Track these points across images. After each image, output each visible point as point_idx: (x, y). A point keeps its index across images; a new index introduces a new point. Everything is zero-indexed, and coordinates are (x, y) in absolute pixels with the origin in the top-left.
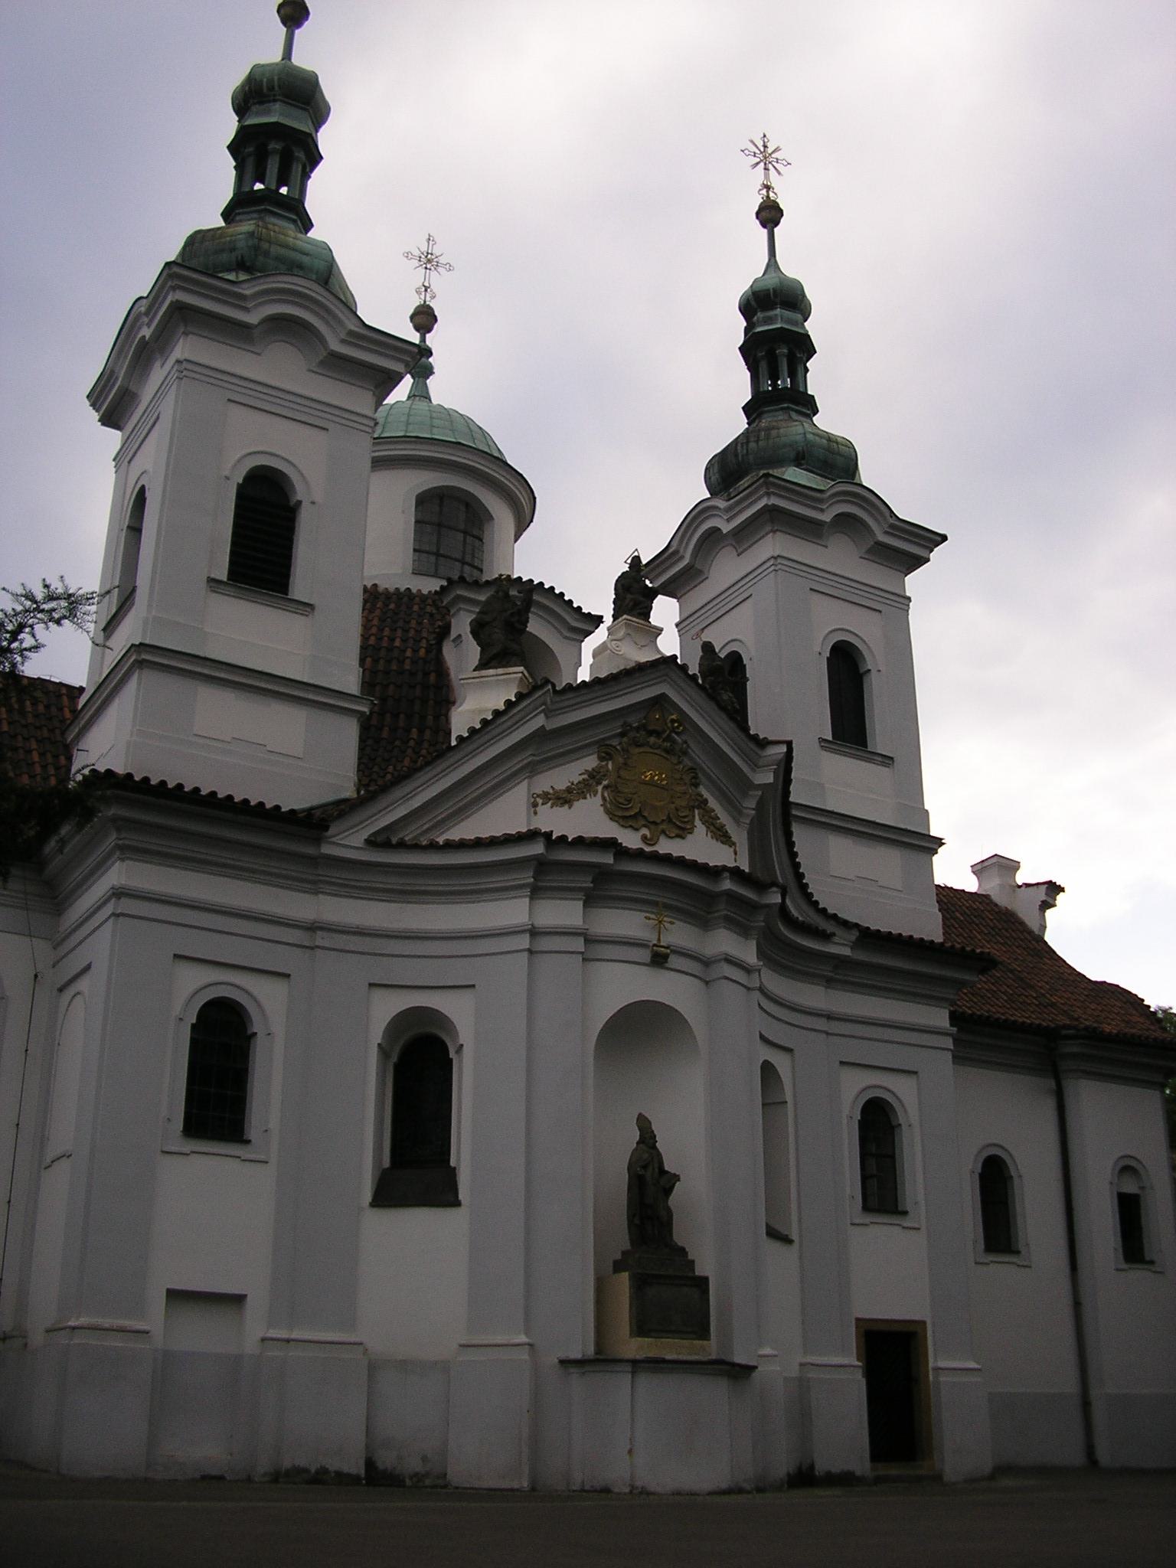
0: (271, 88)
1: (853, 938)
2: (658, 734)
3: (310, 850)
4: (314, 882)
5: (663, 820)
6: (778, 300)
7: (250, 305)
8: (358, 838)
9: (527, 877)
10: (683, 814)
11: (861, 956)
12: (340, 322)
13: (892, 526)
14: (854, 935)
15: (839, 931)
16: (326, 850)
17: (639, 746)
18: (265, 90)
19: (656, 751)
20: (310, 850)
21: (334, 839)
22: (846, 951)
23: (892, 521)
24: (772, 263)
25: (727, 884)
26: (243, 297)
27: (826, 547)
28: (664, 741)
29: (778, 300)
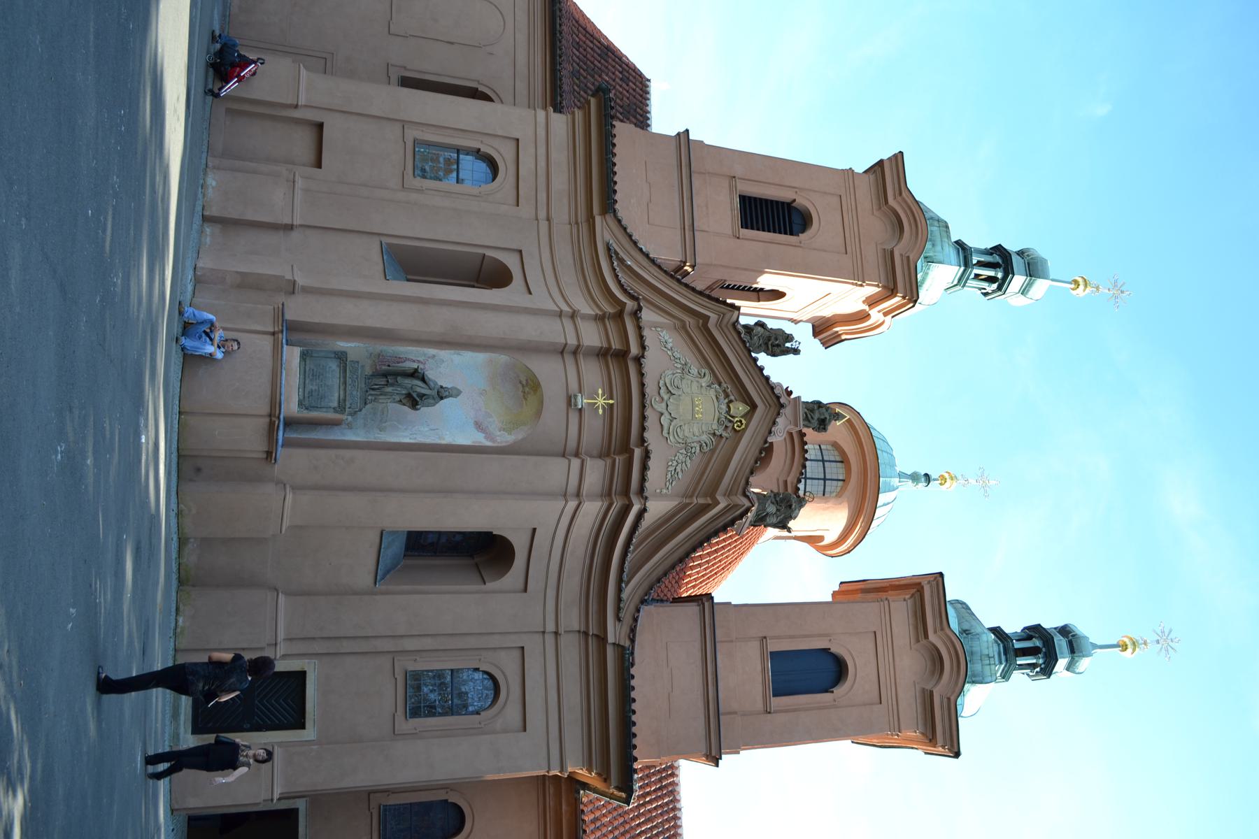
0: (1028, 256)
1: (622, 643)
2: (728, 412)
4: (577, 223)
6: (1070, 638)
7: (899, 198)
8: (608, 237)
9: (609, 309)
13: (949, 699)
15: (625, 629)
16: (598, 219)
17: (717, 398)
18: (1026, 254)
19: (717, 411)
21: (605, 223)
22: (611, 639)
23: (952, 698)
24: (1095, 646)
26: (900, 194)
27: (911, 648)
28: (726, 418)
29: (1070, 638)
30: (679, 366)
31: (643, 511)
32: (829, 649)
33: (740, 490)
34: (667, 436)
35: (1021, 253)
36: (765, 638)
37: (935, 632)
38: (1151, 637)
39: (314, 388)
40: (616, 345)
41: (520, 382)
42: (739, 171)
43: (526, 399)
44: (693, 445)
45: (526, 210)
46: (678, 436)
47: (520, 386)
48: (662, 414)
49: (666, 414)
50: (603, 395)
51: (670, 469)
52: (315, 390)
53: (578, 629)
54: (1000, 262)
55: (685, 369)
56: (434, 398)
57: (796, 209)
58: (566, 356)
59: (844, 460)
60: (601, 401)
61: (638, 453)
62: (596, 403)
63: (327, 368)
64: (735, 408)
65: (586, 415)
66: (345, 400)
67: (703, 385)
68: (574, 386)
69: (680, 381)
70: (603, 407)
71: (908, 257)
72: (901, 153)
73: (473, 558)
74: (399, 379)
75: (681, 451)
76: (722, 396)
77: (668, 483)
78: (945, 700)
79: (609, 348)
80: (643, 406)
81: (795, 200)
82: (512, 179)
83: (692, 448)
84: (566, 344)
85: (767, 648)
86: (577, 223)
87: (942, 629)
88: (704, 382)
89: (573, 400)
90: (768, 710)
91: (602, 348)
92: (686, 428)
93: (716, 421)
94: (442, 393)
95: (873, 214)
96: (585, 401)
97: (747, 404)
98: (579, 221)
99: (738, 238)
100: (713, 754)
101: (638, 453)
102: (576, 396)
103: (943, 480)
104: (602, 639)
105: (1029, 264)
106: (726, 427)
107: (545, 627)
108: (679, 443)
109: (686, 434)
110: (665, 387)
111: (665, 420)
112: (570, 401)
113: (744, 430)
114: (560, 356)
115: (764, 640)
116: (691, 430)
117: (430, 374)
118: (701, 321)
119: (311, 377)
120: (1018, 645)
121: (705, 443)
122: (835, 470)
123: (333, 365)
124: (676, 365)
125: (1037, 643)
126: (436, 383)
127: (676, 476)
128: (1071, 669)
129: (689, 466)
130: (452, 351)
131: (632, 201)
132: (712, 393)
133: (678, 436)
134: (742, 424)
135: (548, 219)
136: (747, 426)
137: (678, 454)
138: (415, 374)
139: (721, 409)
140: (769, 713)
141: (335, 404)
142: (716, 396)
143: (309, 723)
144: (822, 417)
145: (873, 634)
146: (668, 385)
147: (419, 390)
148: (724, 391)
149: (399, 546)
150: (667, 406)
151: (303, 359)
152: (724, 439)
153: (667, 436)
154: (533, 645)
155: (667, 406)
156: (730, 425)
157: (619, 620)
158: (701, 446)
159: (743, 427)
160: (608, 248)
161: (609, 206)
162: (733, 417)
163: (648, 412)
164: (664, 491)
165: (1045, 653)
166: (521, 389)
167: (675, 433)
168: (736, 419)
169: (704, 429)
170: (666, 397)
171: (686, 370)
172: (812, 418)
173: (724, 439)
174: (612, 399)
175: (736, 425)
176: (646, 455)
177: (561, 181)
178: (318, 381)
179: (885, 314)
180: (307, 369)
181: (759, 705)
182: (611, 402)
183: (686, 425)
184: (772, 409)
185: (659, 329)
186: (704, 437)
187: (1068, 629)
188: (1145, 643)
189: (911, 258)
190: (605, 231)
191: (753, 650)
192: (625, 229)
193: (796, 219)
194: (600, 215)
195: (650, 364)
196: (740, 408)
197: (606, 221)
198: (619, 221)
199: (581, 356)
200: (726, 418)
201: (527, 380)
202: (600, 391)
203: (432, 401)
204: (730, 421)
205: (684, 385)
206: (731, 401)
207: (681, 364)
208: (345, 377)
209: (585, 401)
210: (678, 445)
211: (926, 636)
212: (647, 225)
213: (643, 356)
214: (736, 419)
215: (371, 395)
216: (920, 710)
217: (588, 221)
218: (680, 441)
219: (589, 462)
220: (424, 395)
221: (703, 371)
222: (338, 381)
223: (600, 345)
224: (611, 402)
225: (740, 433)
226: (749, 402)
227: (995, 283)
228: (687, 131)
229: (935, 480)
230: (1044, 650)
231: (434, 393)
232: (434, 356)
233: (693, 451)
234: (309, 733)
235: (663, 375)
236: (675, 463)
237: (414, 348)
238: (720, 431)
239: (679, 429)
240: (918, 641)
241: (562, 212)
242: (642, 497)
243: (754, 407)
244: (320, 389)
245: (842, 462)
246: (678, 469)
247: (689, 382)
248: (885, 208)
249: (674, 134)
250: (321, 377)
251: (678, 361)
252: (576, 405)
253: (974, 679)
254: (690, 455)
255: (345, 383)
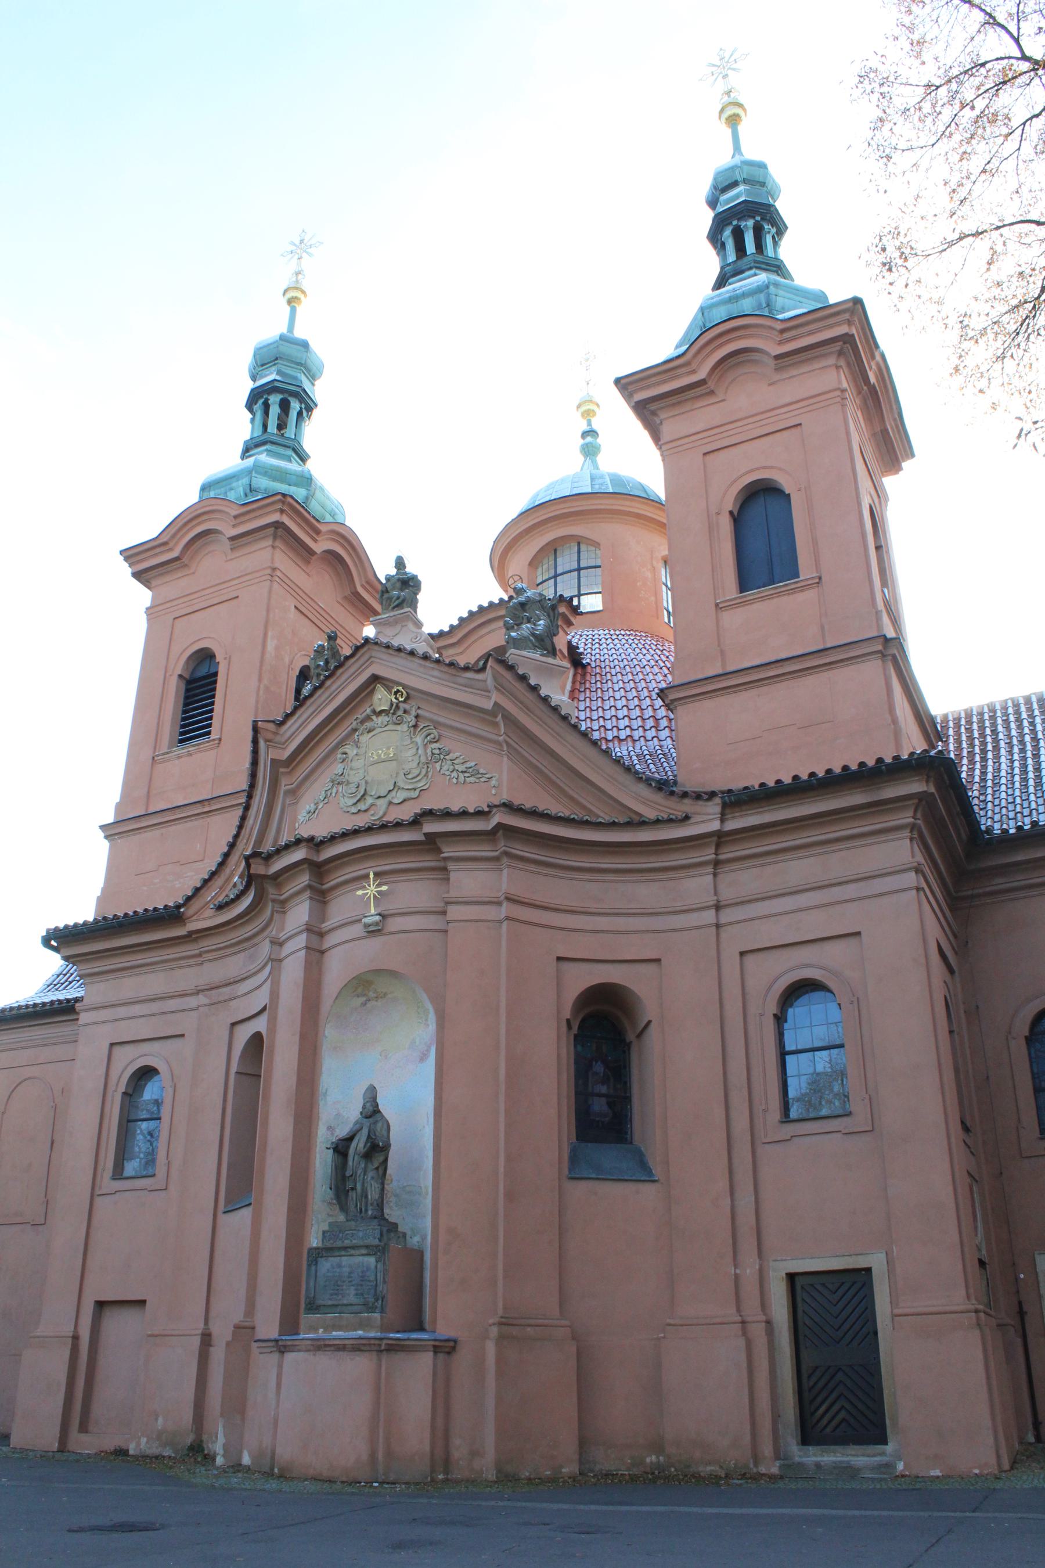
1: (718, 809)
3: (180, 931)
4: (200, 955)
5: (390, 791)
6: (718, 192)
7: (171, 545)
8: (209, 912)
10: (415, 775)
11: (731, 825)
12: (227, 513)
13: (782, 331)
14: (714, 807)
15: (701, 807)
16: (192, 926)
17: (369, 731)
20: (181, 932)
21: (194, 918)
22: (715, 826)
23: (779, 326)
25: (497, 818)
26: (165, 544)
28: (394, 714)
30: (334, 790)
31: (508, 807)
32: (731, 513)
33: (480, 676)
34: (418, 791)
35: (254, 378)
36: (717, 605)
37: (694, 372)
38: (721, 86)
39: (352, 1291)
40: (304, 879)
41: (364, 1004)
42: (147, 754)
43: (385, 994)
44: (429, 751)
45: (187, 1024)
46: (418, 775)
47: (369, 1005)
48: (390, 803)
49: (389, 797)
50: (364, 888)
51: (461, 778)
52: (356, 1290)
53: (711, 876)
54: (261, 401)
55: (338, 781)
56: (376, 1123)
57: (192, 673)
58: (325, 946)
59: (553, 549)
60: (372, 890)
61: (431, 827)
62: (375, 896)
63: (329, 1274)
64: (380, 705)
65: (387, 907)
66: (367, 1247)
67: (355, 752)
68: (357, 930)
69: (351, 786)
70: (379, 885)
71: (235, 517)
72: (122, 552)
73: (631, 1042)
74: (348, 1173)
75: (438, 768)
76: (368, 725)
77: (483, 780)
78: (786, 335)
79: (309, 887)
80: (384, 827)
81: (180, 676)
82: (156, 1046)
83: (433, 754)
84: (307, 947)
85: (735, 599)
86: (200, 955)
87: (688, 364)
88: (352, 751)
89: (372, 928)
90: (817, 580)
91: (311, 898)
92: (407, 767)
93: (399, 728)
94: (372, 1112)
95: (193, 573)
96: (373, 911)
97: (373, 691)
98: (197, 952)
99: (220, 740)
100: (880, 647)
101: (431, 827)
102: (366, 926)
103: (588, 414)
104: (720, 838)
105: (262, 365)
106: (405, 712)
107: (709, 926)
108: (427, 772)
109: (415, 764)
110: (358, 804)
111: (400, 796)
112: (374, 931)
113: (404, 687)
114: (327, 954)
115: (721, 606)
116: (410, 759)
117: (342, 1132)
118: (282, 770)
119: (340, 1297)
120: (732, 257)
121: (427, 737)
122: (566, 560)
123: (326, 1265)
124: (334, 795)
125: (727, 232)
126: (356, 1123)
127: (471, 770)
128: (761, 180)
129: (458, 754)
130: (321, 1103)
131: (177, 886)
132: (364, 738)
133: (418, 775)
134: (398, 691)
135: (198, 992)
136: (398, 684)
137: (442, 772)
138: (341, 1149)
139: (382, 723)
140: (820, 578)
141: (372, 1260)
142: (369, 732)
143: (861, 1263)
144: (398, 585)
145: (708, 457)
146: (355, 801)
147: (361, 1145)
148: (362, 722)
149: (607, 1155)
150: (379, 797)
151: (316, 1309)
152: (419, 712)
153: (418, 791)
154: (735, 940)
155: (379, 797)
156: (401, 705)
157: (687, 818)
158: (431, 742)
159: (400, 688)
160: (220, 907)
161: (171, 916)
162: (392, 705)
163: (390, 818)
164: (493, 782)
165: (739, 220)
166: (373, 1003)
167: (414, 780)
168: (394, 700)
169: (409, 741)
170: (369, 801)
171: (341, 779)
172: (398, 598)
173: (419, 712)
174: (367, 876)
175: (401, 699)
176: (429, 814)
177: (154, 982)
178: (344, 1287)
179: (318, 532)
180: (330, 1303)
181: (811, 594)
182: (372, 876)
183: (404, 766)
184: (374, 654)
185: (297, 825)
186: (419, 739)
187: (710, 199)
188: (728, 93)
189: (234, 513)
190: (203, 918)
191: (733, 619)
192: (197, 890)
193: (203, 671)
194: (185, 925)
195: (320, 831)
196: (382, 698)
197: (192, 916)
198: (189, 899)
199: (324, 925)
200: (394, 714)
201: (358, 996)
202: (360, 893)
203: (379, 1125)
204: (398, 707)
205: (355, 778)
206: (374, 712)
207: (332, 787)
208: (340, 1249)
209: (373, 911)
210: (430, 774)
211: (702, 382)
212: (205, 861)
213: (311, 839)
214: (394, 700)
215: (366, 1210)
216: (805, 368)
217: (196, 940)
218: (424, 771)
219: (454, 894)
220: (369, 1136)
221: (339, 756)
222: (346, 1258)
223: (308, 901)
224: (372, 876)
225: (408, 691)
226: (372, 686)
227: (289, 403)
228: (103, 827)
229: (589, 423)
230: (735, 223)
231: (366, 1123)
232: (330, 1128)
233: (437, 752)
234: (876, 1261)
235: (345, 809)
236: (455, 774)
237: (318, 1156)
238: (411, 719)
239: (410, 776)
240: (712, 393)
241: (189, 977)
242: (489, 812)
243: (375, 679)
244: (353, 1283)
245: (555, 551)
246: (461, 768)
247: (352, 773)
248: (185, 560)
249: (106, 844)
250: (339, 1283)
251: (329, 793)
252: (377, 924)
253: (764, 305)
254: (444, 753)
255: (345, 1248)
